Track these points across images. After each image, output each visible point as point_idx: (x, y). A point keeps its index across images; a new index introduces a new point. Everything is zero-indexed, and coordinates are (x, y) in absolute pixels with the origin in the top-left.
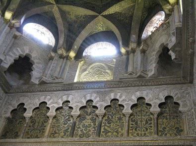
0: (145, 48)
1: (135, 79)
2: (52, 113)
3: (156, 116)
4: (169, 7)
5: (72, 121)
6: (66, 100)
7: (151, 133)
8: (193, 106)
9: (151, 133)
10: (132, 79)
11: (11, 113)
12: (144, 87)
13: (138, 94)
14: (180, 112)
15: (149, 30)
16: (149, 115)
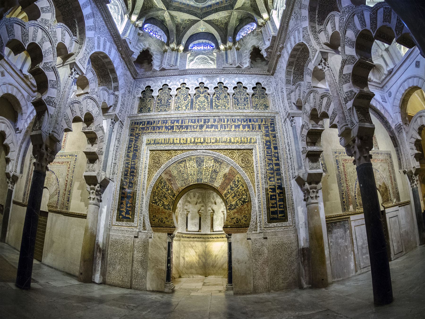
0: (239, 47)
1: (234, 69)
2: (174, 92)
3: (251, 96)
4: (262, 21)
5: (190, 98)
6: (182, 82)
7: (248, 107)
8: (274, 91)
9: (248, 107)
10: (232, 68)
11: (142, 93)
12: (241, 75)
13: (237, 80)
14: (266, 94)
15: (241, 34)
16: (246, 95)
